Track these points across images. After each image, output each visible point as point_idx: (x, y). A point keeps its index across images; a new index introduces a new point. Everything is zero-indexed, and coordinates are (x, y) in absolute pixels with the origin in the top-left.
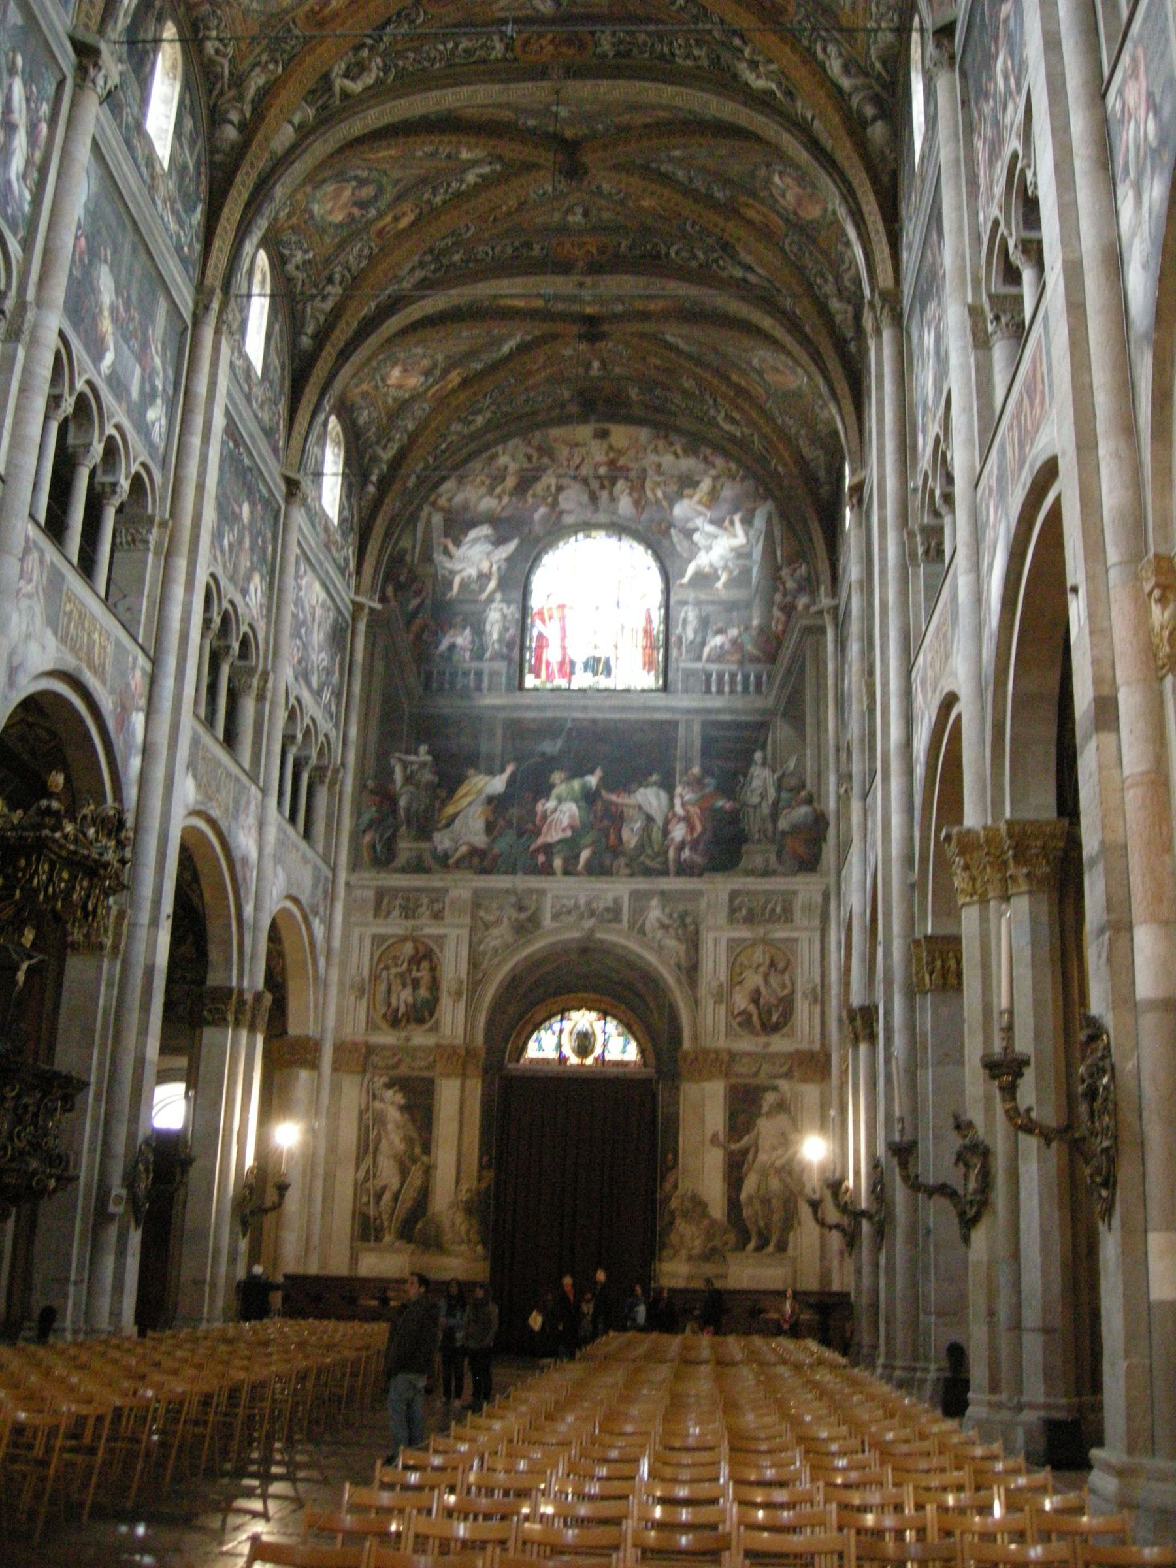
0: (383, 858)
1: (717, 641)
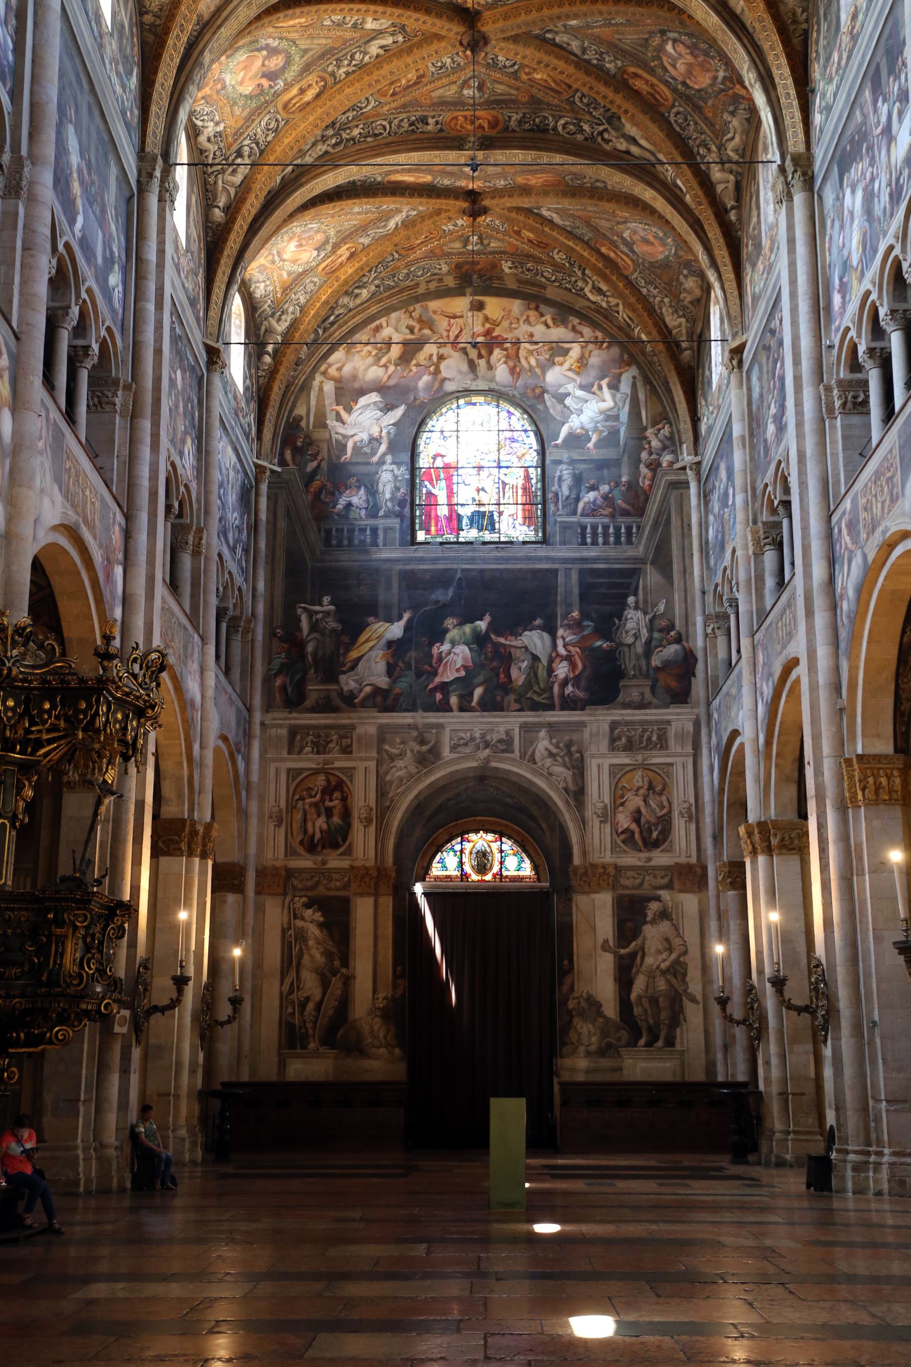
0: (294, 700)
1: (591, 495)
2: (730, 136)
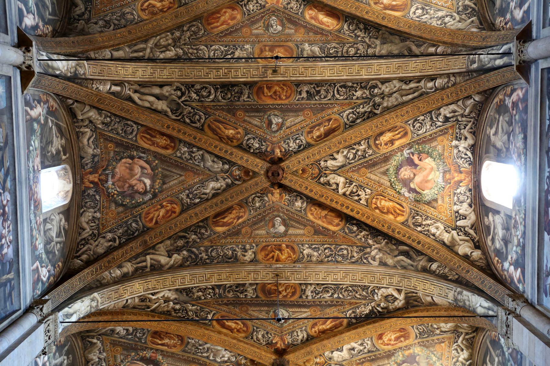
2: (92, 140)
